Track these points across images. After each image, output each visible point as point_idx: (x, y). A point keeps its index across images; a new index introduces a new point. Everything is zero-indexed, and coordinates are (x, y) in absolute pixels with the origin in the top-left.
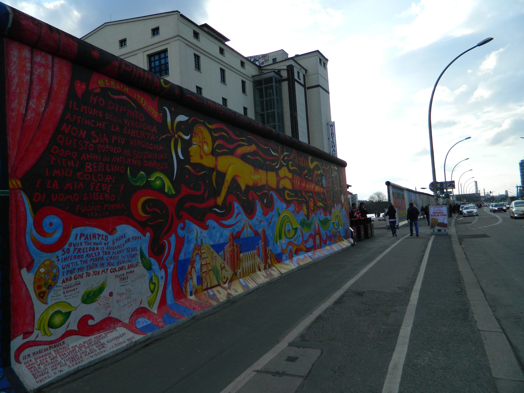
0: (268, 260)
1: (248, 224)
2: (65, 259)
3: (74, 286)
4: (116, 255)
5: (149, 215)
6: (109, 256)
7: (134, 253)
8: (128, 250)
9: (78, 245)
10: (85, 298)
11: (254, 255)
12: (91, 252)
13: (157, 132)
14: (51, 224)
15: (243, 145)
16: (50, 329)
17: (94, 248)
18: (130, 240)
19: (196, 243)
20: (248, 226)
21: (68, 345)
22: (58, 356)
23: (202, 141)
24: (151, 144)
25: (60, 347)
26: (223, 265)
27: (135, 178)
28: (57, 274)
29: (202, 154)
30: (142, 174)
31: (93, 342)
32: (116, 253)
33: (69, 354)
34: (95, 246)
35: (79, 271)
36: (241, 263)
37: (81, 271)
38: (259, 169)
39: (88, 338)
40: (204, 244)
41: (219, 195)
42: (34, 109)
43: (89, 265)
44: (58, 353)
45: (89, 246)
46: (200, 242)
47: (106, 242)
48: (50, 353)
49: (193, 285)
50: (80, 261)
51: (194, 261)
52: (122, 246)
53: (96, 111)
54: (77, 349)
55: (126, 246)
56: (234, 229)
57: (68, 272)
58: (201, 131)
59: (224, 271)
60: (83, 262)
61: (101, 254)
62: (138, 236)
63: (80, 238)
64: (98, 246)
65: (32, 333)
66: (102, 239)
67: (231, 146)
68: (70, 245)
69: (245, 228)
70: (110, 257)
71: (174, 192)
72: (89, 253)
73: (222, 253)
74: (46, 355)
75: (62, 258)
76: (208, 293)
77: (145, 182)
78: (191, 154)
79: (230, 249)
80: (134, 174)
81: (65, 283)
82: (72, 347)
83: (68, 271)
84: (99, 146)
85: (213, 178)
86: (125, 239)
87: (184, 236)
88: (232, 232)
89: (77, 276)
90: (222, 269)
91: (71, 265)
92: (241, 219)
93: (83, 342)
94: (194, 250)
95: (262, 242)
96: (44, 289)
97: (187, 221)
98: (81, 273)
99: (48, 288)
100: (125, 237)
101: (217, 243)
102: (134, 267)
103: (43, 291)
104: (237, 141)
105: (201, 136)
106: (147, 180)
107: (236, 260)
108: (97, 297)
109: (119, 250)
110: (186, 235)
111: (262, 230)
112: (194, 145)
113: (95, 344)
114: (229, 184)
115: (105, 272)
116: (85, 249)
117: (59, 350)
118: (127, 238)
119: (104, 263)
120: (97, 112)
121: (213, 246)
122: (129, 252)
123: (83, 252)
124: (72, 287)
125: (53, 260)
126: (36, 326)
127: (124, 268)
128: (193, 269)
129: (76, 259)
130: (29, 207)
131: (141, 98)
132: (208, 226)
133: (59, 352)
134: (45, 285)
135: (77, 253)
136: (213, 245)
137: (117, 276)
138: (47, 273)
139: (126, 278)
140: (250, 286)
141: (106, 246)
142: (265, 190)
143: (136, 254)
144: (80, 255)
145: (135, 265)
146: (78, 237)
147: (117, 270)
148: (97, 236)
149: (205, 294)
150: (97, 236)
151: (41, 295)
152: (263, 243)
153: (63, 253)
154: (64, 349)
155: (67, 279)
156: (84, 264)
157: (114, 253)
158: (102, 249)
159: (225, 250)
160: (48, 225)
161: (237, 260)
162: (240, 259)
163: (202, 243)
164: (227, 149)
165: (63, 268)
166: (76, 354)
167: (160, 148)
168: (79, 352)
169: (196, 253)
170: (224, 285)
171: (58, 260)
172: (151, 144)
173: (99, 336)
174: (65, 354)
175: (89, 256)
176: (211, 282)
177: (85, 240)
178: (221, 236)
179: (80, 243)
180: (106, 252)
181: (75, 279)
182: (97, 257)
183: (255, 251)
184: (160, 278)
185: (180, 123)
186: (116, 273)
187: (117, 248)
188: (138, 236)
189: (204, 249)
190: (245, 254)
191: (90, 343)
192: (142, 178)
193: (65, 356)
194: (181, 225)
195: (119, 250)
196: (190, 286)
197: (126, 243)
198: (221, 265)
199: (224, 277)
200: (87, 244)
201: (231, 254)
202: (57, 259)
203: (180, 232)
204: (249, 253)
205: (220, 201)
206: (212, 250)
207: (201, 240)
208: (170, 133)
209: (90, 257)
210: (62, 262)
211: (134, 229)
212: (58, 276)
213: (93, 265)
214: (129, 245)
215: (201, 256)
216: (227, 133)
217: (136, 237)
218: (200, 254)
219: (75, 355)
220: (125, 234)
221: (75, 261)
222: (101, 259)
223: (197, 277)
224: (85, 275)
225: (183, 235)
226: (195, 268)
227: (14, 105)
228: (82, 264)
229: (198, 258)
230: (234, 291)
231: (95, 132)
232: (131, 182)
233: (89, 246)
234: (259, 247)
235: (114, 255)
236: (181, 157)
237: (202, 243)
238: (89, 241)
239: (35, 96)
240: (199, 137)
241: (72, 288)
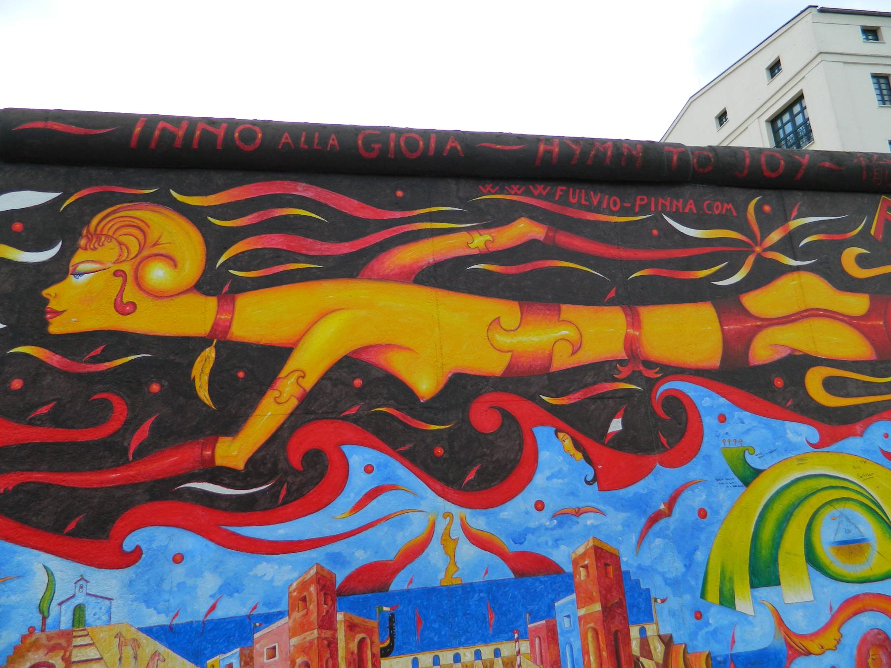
23: (136, 256)
78: (53, 305)
79: (294, 641)
105: (123, 239)
132: (137, 553)
178: (230, 588)
240: (121, 244)
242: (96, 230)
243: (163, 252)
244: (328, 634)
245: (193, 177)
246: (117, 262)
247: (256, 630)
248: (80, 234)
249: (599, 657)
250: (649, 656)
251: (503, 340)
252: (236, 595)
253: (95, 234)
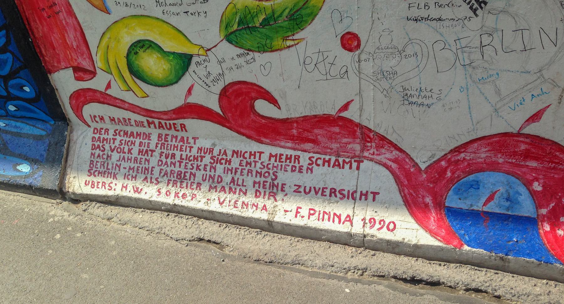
21: (195, 139)
22: (158, 150)
25: (172, 132)
31: (259, 165)
33: (180, 162)
39: (254, 146)
44: (163, 144)
48: (148, 136)
54: (207, 160)
74: (138, 135)
82: (200, 149)
93: (234, 151)
113: (257, 172)
117: (169, 138)
133: (165, 144)
154: (181, 143)
166: (194, 171)
168: (205, 170)
173: (289, 158)
174: (173, 156)
191: (248, 164)
193: (169, 163)
219: (191, 173)
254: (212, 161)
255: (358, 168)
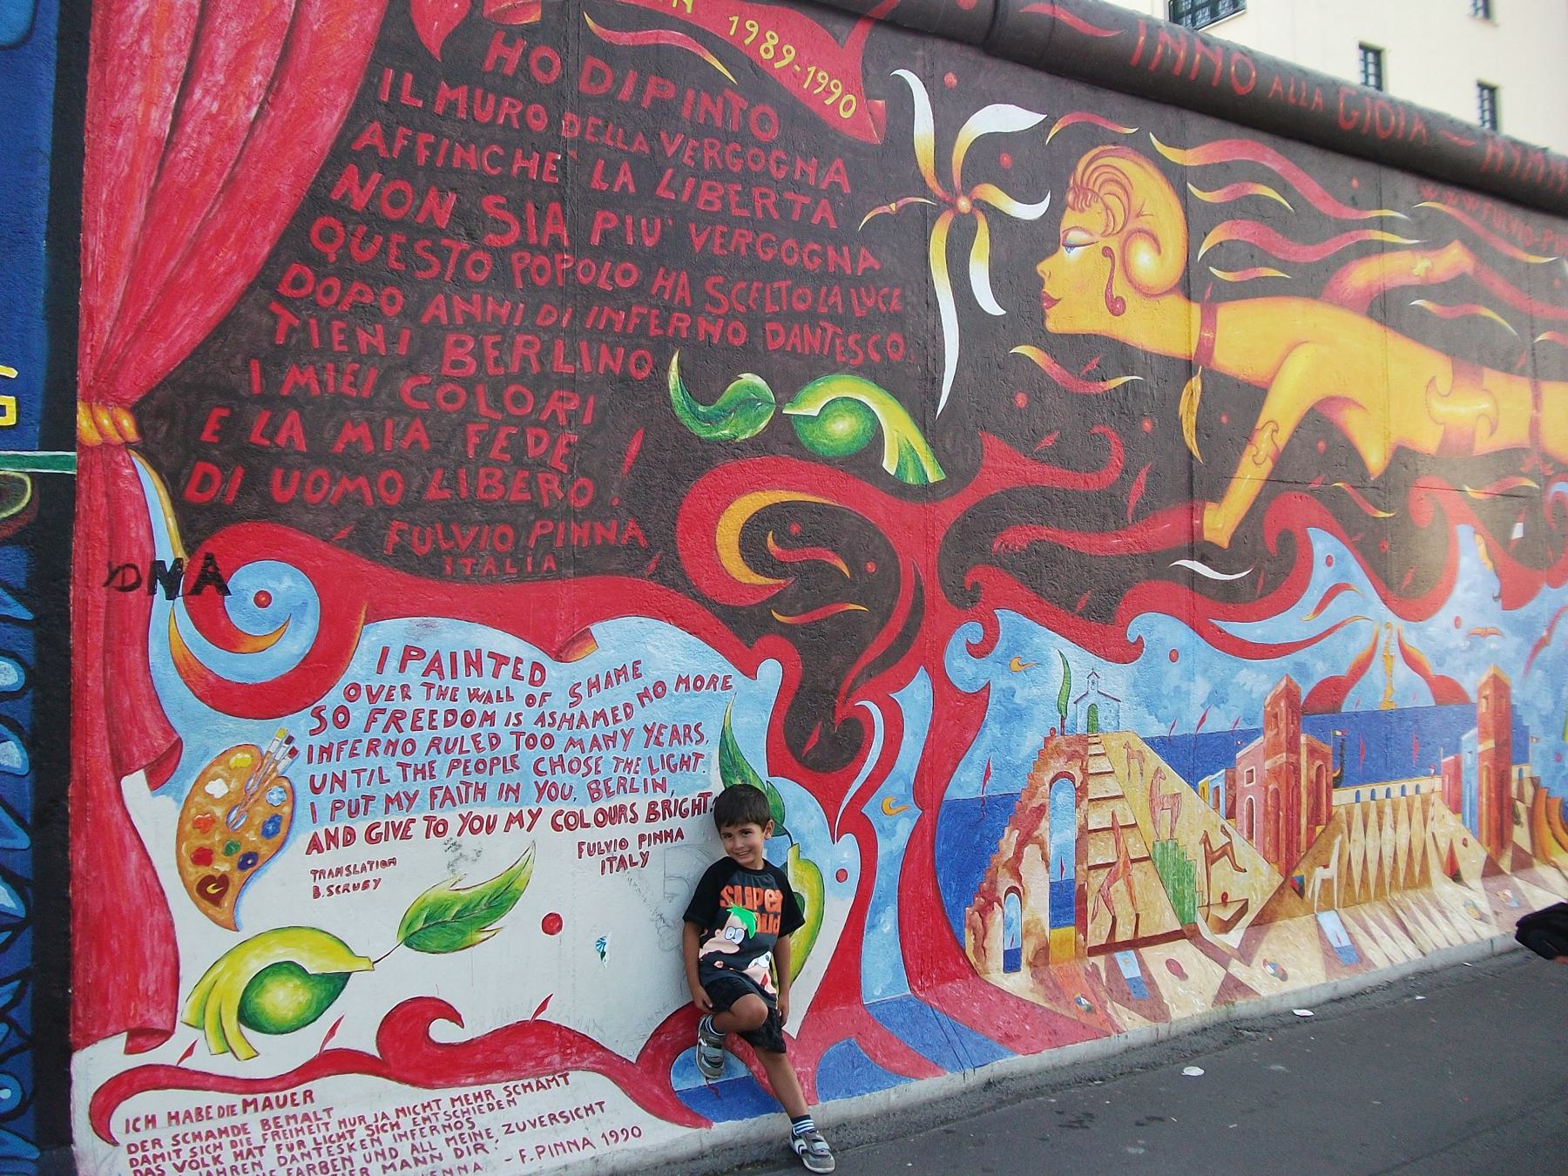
0: (1516, 829)
1: (1394, 641)
2: (326, 751)
3: (364, 868)
4: (583, 752)
5: (782, 581)
6: (547, 754)
7: (689, 749)
8: (655, 733)
9: (389, 698)
10: (420, 925)
11: (1426, 802)
12: (457, 730)
13: (847, 190)
14: (263, 599)
15: (1384, 248)
16: (248, 1032)
17: (470, 713)
18: (664, 690)
19: (1058, 726)
20: (1395, 650)
21: (328, 1110)
22: (271, 1145)
23: (1121, 230)
24: (816, 247)
25: (289, 1110)
26: (1218, 841)
27: (709, 400)
28: (287, 810)
29: (1120, 290)
30: (755, 389)
31: (441, 1116)
32: (587, 747)
33: (318, 1150)
34: (479, 708)
35: (394, 807)
36: (1340, 837)
37: (400, 806)
38: (1487, 372)
39: (426, 1095)
40: (1109, 729)
41: (1217, 491)
42: (211, 117)
43: (440, 788)
44: (275, 1134)
45: (448, 704)
46: (1082, 721)
47: (537, 692)
48: (244, 1129)
49: (1028, 923)
50: (399, 764)
51: (1040, 811)
52: (621, 714)
53: (513, 106)
54: (361, 1132)
55: (642, 716)
56: (1301, 668)
57: (338, 809)
58: (1124, 181)
59: (1222, 868)
60: (410, 772)
61: (508, 742)
62: (714, 676)
63: (402, 668)
64: (489, 708)
65: (167, 1034)
66: (516, 676)
67: (1308, 254)
68: (352, 692)
69: (1376, 668)
70: (556, 760)
71: (934, 474)
72: (443, 732)
73: (1217, 779)
74: (222, 1132)
75: (311, 747)
76: (1113, 968)
77: (763, 425)
78: (1050, 289)
79: (1268, 764)
80: (702, 387)
81: (320, 851)
82: (342, 1122)
83: (338, 805)
84: (521, 258)
85: (1183, 408)
86: (638, 685)
87: (987, 687)
88: (1290, 681)
89: (382, 829)
90: (1211, 858)
91: (351, 779)
92: (1355, 618)
93: (397, 1110)
94: (1044, 754)
95: (1483, 736)
96: (221, 866)
97: (1005, 617)
98: (398, 817)
99: (243, 866)
100: (637, 676)
101: (1193, 732)
102: (683, 816)
103: (217, 875)
104: (1343, 227)
105: (1112, 201)
106: (778, 413)
107: (1304, 821)
108: (481, 930)
109: (600, 730)
110: (1000, 683)
111: (1484, 678)
112: (1072, 247)
113: (444, 1126)
114: (1282, 438)
115: (522, 826)
116: (425, 716)
117: (282, 1121)
118: (648, 681)
119: (518, 785)
120: (519, 109)
121: (1161, 745)
122: (660, 744)
123: (414, 728)
124: (356, 872)
125: (268, 752)
126: (186, 1009)
127: (630, 815)
128: (1031, 851)
129: (376, 754)
130: (167, 523)
131: (768, 35)
133: (278, 1132)
134: (228, 852)
135: (386, 729)
136: (1162, 738)
137: (585, 847)
138: (241, 800)
139: (637, 858)
140: (1373, 953)
141: (535, 711)
142: (1523, 475)
143: (698, 756)
144: (397, 741)
145: (688, 805)
146: (393, 662)
147: (589, 819)
148: (488, 665)
149: (1094, 973)
150: (488, 665)
151: (211, 890)
152: (1491, 744)
153: (316, 723)
154: (307, 1123)
155: (332, 838)
156: (415, 779)
157: (572, 742)
158: (513, 720)
159: (1239, 768)
160: (251, 601)
161: (1314, 819)
162: (1330, 818)
163: (1092, 725)
164: (1283, 265)
165: (316, 791)
166: (346, 1154)
167: (862, 266)
168: (363, 1147)
169: (1052, 775)
170: (1222, 937)
171: (293, 753)
172: (816, 247)
173: (478, 1097)
174: (301, 1144)
175: (442, 747)
176: (1138, 916)
177: (426, 674)
178: (1217, 698)
179: (398, 689)
180: (533, 736)
181: (369, 840)
182: (487, 755)
183: (1432, 784)
184: (829, 878)
185: (990, 144)
186: (581, 834)
187: (590, 722)
188: (714, 676)
189: (1104, 754)
190: (1365, 791)
191: (424, 1120)
192: (748, 403)
193: (299, 1157)
194: (972, 631)
195: (600, 730)
196: (1008, 925)
197: (643, 704)
198: (1206, 840)
199: (1225, 896)
200: (434, 692)
201: (1271, 787)
202: (287, 748)
203: (962, 669)
204: (1395, 788)
205: (1219, 522)
206: (1155, 760)
207: (1093, 709)
208: (925, 191)
209: (448, 751)
210: (310, 761)
211: (693, 638)
212: (291, 820)
213: (463, 788)
214: (656, 712)
215: (1081, 791)
216: (1284, 188)
217: (699, 678)
218: (1079, 779)
219: (344, 1159)
220: (638, 662)
221: (372, 762)
222: (505, 766)
223: (1052, 885)
224: (419, 828)
225: (982, 683)
226: (1042, 845)
227: (129, 107)
228: (405, 779)
229: (1064, 796)
230: (1270, 969)
231: (503, 201)
232: (687, 420)
233: (448, 704)
234: (1457, 764)
235: (575, 752)
236: (989, 304)
237: (1092, 725)
238: (448, 683)
239: (220, 61)
240: (1107, 208)
241: (359, 879)
242: (1087, 184)
243: (1146, 227)
244: (1293, 759)
245: (1171, 115)
246: (1105, 234)
247: (1239, 749)
248: (1068, 183)
249: (1489, 799)
250: (1522, 801)
251: (1441, 408)
252: (1222, 705)
253: (1082, 188)
254: (370, 1132)
255: (567, 1083)
